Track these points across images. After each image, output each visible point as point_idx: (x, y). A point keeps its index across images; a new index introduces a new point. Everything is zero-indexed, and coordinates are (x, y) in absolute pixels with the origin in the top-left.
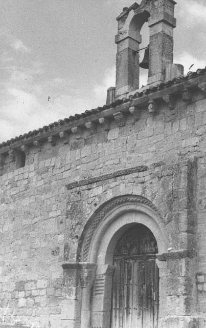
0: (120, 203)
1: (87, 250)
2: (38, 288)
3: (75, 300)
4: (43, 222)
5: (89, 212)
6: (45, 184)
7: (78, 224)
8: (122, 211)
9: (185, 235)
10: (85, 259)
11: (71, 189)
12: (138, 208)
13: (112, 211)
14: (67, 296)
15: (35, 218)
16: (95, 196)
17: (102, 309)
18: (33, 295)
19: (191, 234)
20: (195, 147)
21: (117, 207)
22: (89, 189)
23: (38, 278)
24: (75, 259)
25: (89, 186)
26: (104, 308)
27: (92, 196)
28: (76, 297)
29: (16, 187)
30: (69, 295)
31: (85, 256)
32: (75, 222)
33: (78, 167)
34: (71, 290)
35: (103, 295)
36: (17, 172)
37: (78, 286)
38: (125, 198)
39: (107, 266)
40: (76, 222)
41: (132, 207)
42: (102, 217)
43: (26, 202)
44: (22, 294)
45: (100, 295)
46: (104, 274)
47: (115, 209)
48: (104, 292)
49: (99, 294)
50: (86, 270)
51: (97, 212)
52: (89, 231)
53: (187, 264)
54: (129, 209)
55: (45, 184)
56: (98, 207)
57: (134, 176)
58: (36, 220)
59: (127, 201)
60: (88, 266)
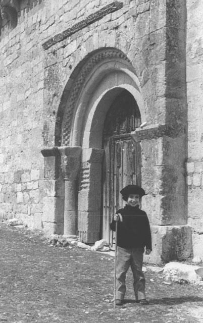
0: (97, 62)
1: (68, 130)
2: (31, 179)
3: (55, 196)
4: (34, 96)
6: (33, 46)
7: (55, 95)
8: (102, 73)
9: (163, 101)
10: (66, 142)
14: (48, 192)
15: (27, 92)
16: (70, 55)
17: (87, 209)
18: (28, 188)
19: (173, 100)
22: (64, 47)
23: (32, 168)
24: (53, 143)
26: (90, 206)
27: (67, 55)
28: (56, 194)
29: (11, 54)
32: (52, 93)
33: (61, 18)
34: (50, 183)
35: (88, 189)
36: (11, 35)
37: (59, 179)
38: (100, 53)
39: (91, 149)
41: (110, 66)
42: (82, 84)
43: (18, 72)
44: (19, 187)
46: (89, 161)
47: (94, 69)
48: (89, 185)
50: (66, 157)
51: (73, 77)
52: (69, 103)
53: (166, 146)
55: (33, 46)
56: (73, 69)
58: (28, 93)
59: (103, 58)
60: (68, 151)
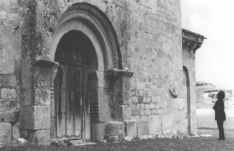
5: (63, 6)
14: (42, 101)
21: (75, 11)
30: (44, 100)
54: (85, 17)
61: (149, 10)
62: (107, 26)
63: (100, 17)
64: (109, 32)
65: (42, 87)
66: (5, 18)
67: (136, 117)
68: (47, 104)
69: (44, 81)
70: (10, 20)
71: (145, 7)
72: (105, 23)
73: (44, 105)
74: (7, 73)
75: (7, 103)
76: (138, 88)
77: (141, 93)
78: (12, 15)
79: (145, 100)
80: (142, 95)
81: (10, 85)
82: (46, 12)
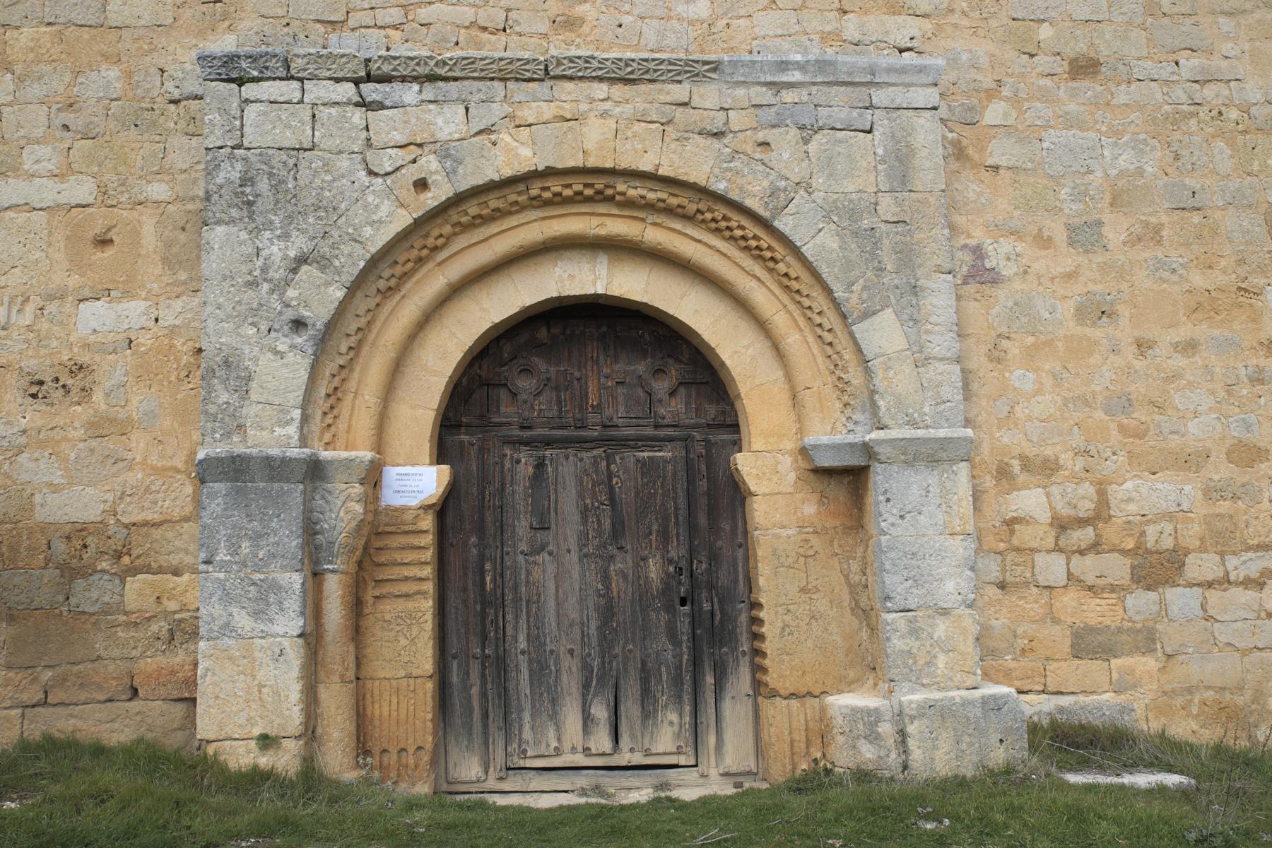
0: (559, 200)
11: (240, 82)
12: (654, 235)
13: (494, 228)
14: (243, 621)
16: (420, 145)
20: (901, 51)
21: (534, 214)
25: (372, 91)
30: (257, 614)
31: (329, 420)
32: (277, 251)
34: (276, 587)
40: (292, 254)
42: (435, 249)
45: (411, 605)
49: (407, 596)
52: (362, 304)
54: (602, 232)
57: (663, 98)
61: (1208, 92)
62: (755, 237)
63: (692, 208)
64: (781, 267)
65: (244, 564)
66: (143, 321)
67: (1114, 662)
68: (279, 629)
69: (257, 538)
70: (166, 324)
71: (1167, 82)
72: (741, 227)
73: (263, 638)
74: (157, 517)
75: (154, 628)
76: (1132, 508)
77: (1159, 536)
78: (178, 305)
79: (1202, 566)
80: (1168, 543)
81: (174, 560)
82: (259, 263)
